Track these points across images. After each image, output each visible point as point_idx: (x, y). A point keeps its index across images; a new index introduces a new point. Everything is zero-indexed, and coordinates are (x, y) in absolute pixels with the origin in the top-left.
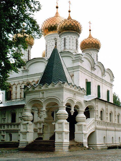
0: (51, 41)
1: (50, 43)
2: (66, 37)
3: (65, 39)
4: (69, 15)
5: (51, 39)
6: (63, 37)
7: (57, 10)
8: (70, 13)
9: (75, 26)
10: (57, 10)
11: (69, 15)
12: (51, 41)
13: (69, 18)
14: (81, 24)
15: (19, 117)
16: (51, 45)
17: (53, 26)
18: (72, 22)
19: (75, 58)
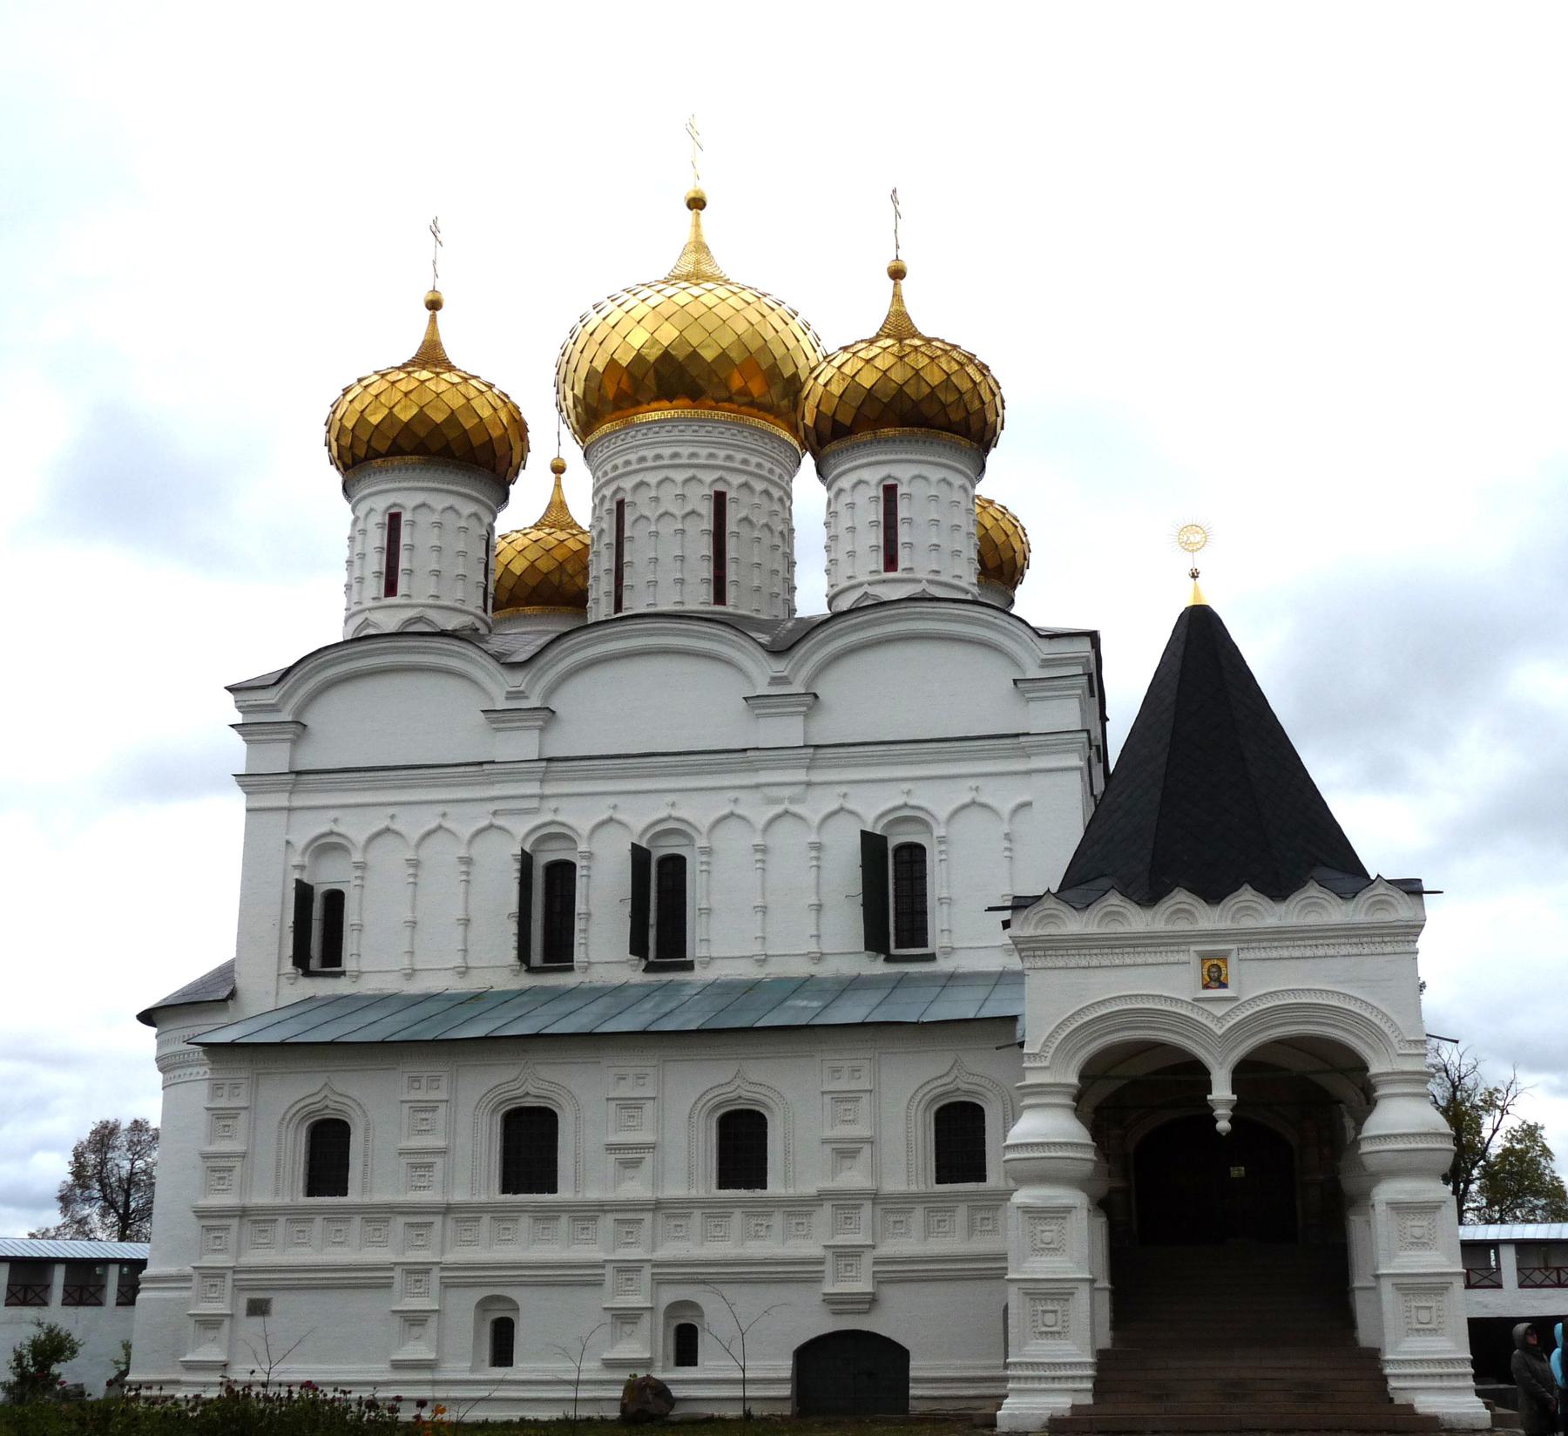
0: (680, 476)
1: (668, 492)
2: (902, 473)
3: (890, 492)
4: (897, 297)
5: (675, 455)
6: (874, 476)
7: (697, 225)
8: (903, 282)
9: (977, 404)
10: (697, 225)
11: (897, 297)
12: (672, 474)
13: (899, 326)
14: (1005, 392)
15: (612, 1148)
16: (653, 515)
17: (709, 355)
18: (932, 359)
19: (1046, 663)
